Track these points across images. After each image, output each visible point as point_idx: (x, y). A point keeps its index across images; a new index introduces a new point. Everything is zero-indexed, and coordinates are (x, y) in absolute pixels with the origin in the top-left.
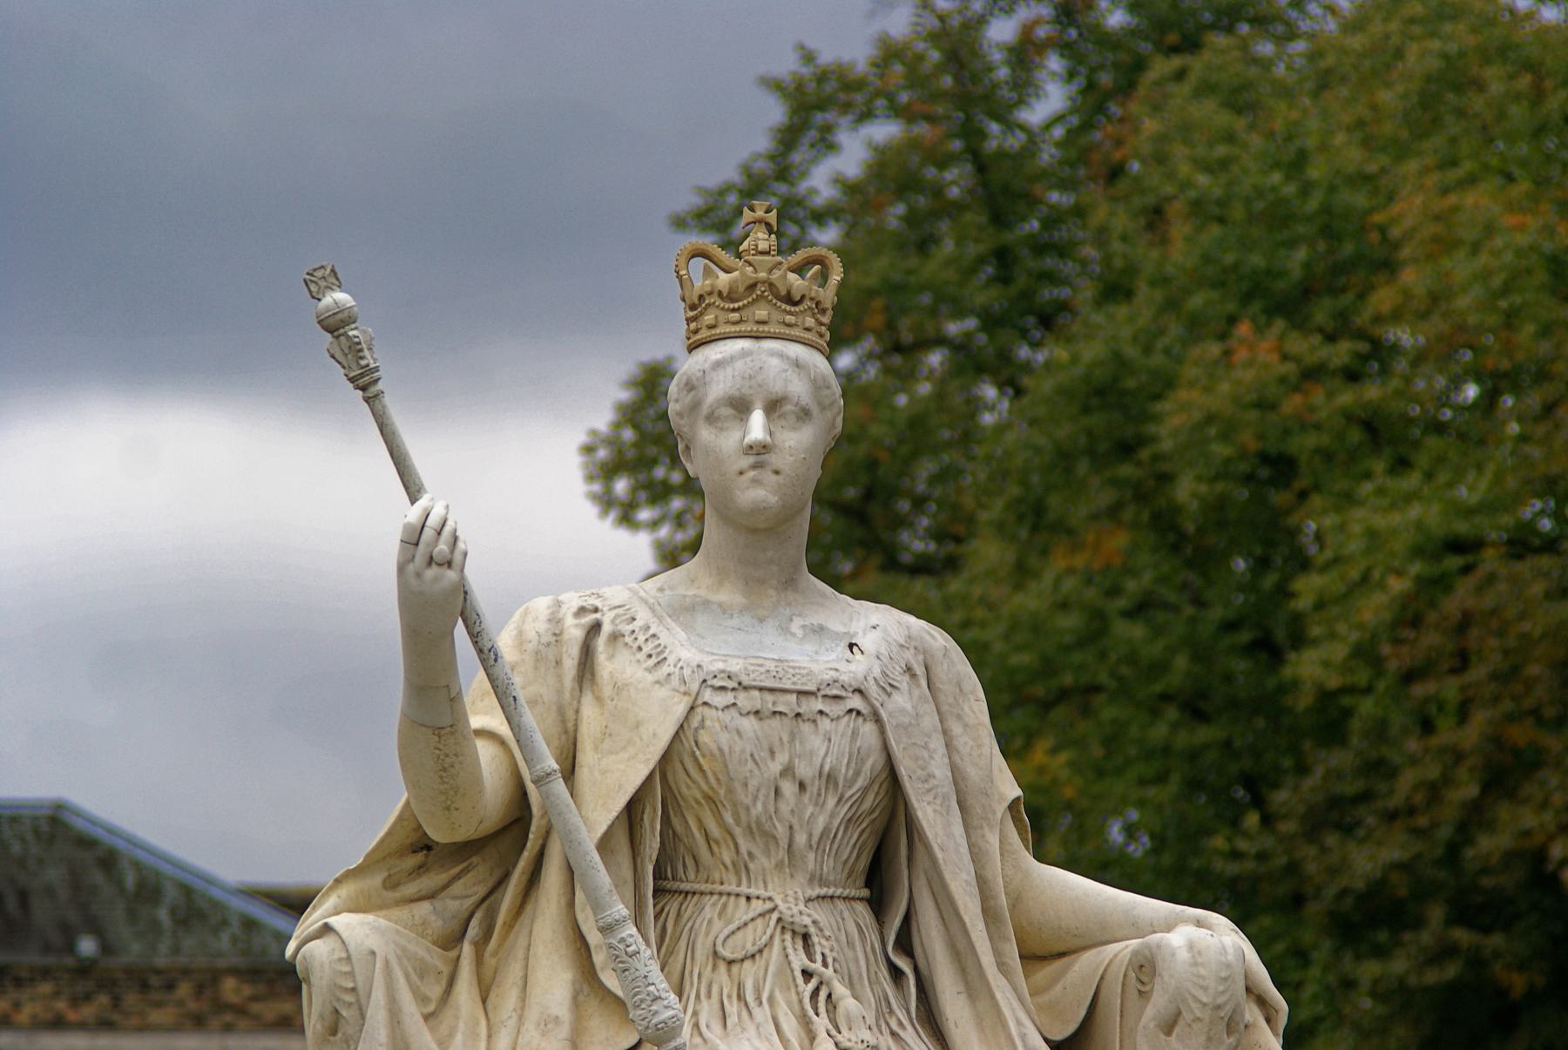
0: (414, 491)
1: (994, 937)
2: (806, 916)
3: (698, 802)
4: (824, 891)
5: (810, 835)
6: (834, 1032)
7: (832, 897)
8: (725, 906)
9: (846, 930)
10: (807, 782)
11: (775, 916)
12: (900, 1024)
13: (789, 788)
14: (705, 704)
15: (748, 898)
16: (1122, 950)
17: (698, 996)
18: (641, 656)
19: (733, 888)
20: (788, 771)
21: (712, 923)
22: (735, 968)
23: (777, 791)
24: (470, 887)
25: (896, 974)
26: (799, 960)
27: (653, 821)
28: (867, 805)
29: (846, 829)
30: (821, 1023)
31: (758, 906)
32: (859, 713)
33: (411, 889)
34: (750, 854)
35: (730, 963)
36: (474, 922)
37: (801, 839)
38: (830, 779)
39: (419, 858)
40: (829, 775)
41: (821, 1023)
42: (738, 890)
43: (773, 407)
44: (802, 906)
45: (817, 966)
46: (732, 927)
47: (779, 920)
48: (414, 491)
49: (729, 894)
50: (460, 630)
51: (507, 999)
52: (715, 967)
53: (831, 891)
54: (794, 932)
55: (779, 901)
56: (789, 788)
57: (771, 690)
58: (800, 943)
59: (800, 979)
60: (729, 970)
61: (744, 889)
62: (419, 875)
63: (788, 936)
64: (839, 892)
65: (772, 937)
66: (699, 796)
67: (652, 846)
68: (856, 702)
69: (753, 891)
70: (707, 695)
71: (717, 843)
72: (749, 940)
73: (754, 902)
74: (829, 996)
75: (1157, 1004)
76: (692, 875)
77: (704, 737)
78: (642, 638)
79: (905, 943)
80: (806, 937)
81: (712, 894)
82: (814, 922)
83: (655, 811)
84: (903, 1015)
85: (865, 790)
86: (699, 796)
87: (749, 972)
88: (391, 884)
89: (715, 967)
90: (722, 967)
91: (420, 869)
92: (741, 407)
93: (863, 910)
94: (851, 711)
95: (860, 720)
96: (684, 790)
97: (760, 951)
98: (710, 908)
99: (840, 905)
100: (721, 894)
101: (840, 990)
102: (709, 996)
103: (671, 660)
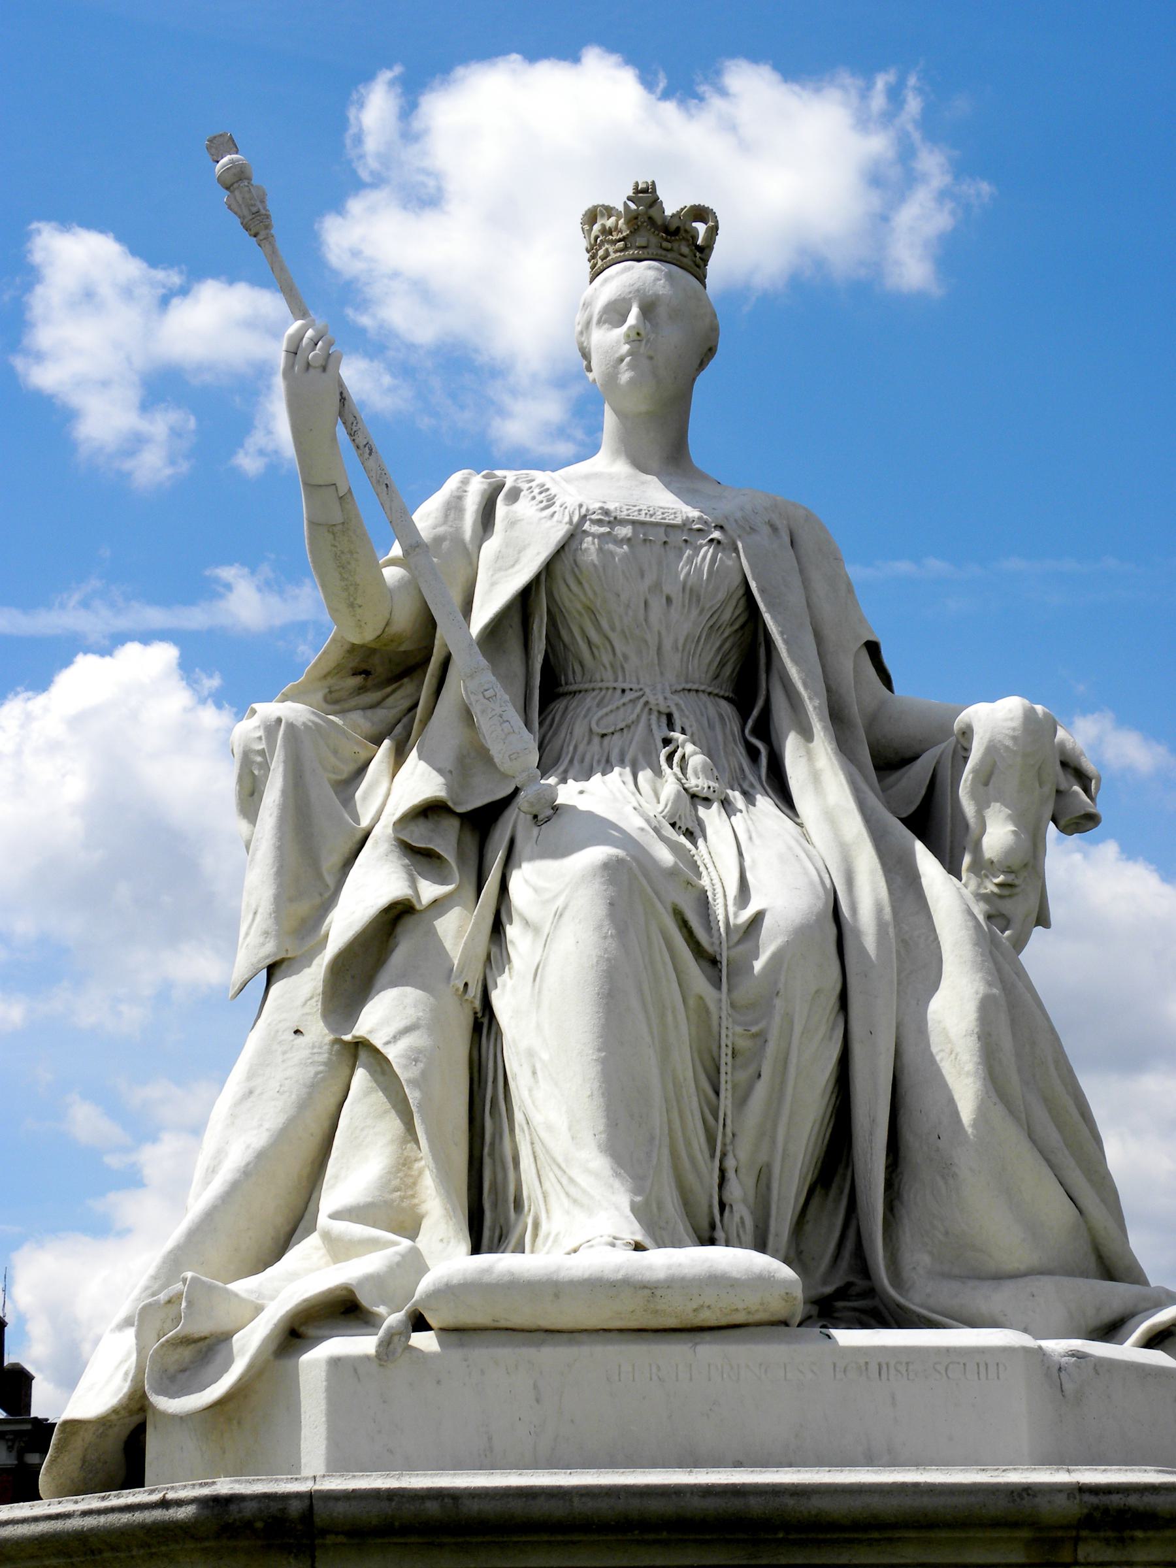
3: (580, 614)
4: (688, 686)
5: (676, 641)
6: (684, 781)
7: (697, 691)
8: (604, 697)
10: (673, 596)
11: (642, 701)
12: (752, 786)
13: (657, 605)
14: (584, 531)
15: (623, 691)
17: (571, 761)
18: (534, 502)
19: (611, 684)
20: (657, 587)
22: (606, 740)
23: (646, 603)
25: (753, 754)
26: (660, 732)
27: (540, 627)
28: (727, 616)
29: (708, 636)
31: (629, 696)
32: (719, 542)
33: (353, 702)
34: (625, 657)
35: (603, 736)
36: (399, 726)
37: (668, 644)
38: (692, 593)
39: (358, 680)
40: (691, 590)
42: (615, 685)
44: (668, 695)
45: (676, 735)
46: (605, 711)
47: (647, 703)
49: (607, 689)
52: (589, 742)
53: (695, 687)
54: (659, 712)
55: (647, 690)
56: (657, 605)
57: (643, 523)
58: (664, 720)
59: (660, 744)
60: (601, 743)
61: (620, 685)
62: (359, 694)
63: (654, 717)
64: (703, 688)
65: (639, 717)
66: (579, 607)
68: (716, 534)
69: (626, 686)
70: (587, 526)
71: (598, 648)
73: (627, 692)
74: (684, 756)
76: (579, 677)
78: (537, 491)
80: (669, 716)
81: (593, 690)
82: (677, 705)
83: (541, 620)
85: (724, 603)
86: (579, 607)
87: (616, 742)
89: (589, 742)
90: (596, 740)
91: (362, 689)
93: (727, 708)
94: (712, 540)
95: (721, 547)
96: (567, 604)
97: (628, 727)
98: (589, 701)
99: (704, 697)
100: (601, 689)
102: (582, 761)
103: (558, 504)
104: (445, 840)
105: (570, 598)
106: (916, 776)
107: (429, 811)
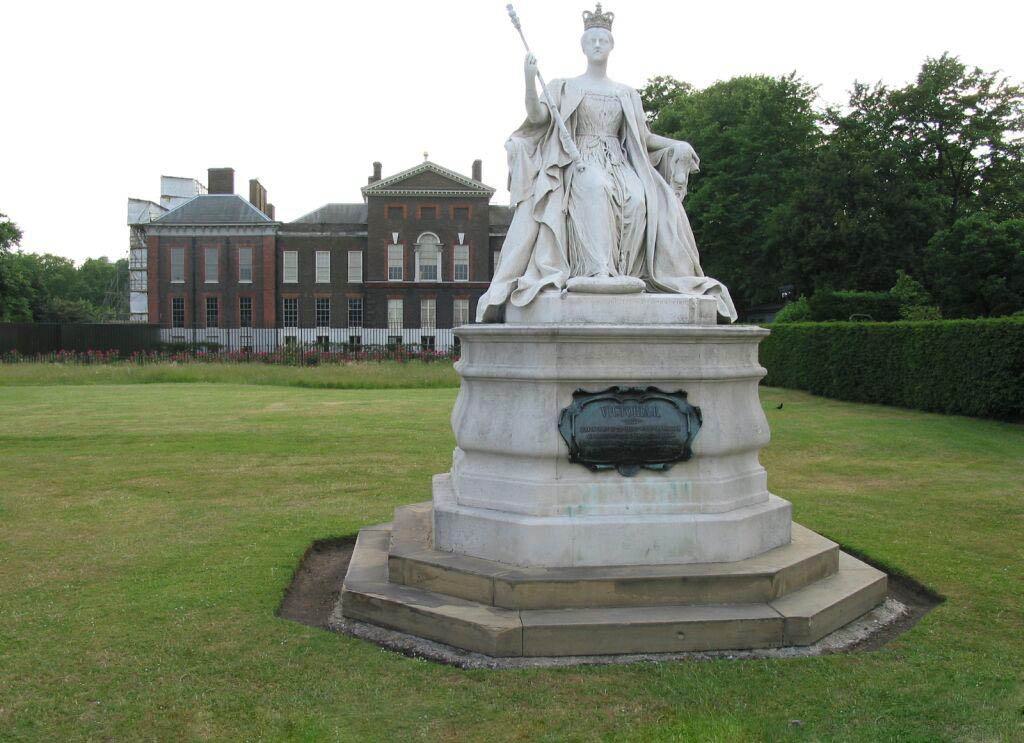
0: (528, 49)
1: (643, 145)
2: (605, 139)
9: (614, 144)
13: (603, 115)
16: (667, 149)
21: (586, 141)
24: (539, 135)
25: (623, 151)
26: (604, 148)
30: (607, 159)
41: (607, 159)
43: (601, 40)
48: (528, 49)
50: (536, 77)
51: (546, 156)
67: (575, 126)
72: (594, 144)
75: (674, 159)
77: (587, 104)
79: (625, 145)
84: (624, 158)
88: (524, 133)
92: (594, 41)
101: (612, 154)
104: (557, 173)
105: (583, 113)
106: (659, 154)
107: (555, 166)
